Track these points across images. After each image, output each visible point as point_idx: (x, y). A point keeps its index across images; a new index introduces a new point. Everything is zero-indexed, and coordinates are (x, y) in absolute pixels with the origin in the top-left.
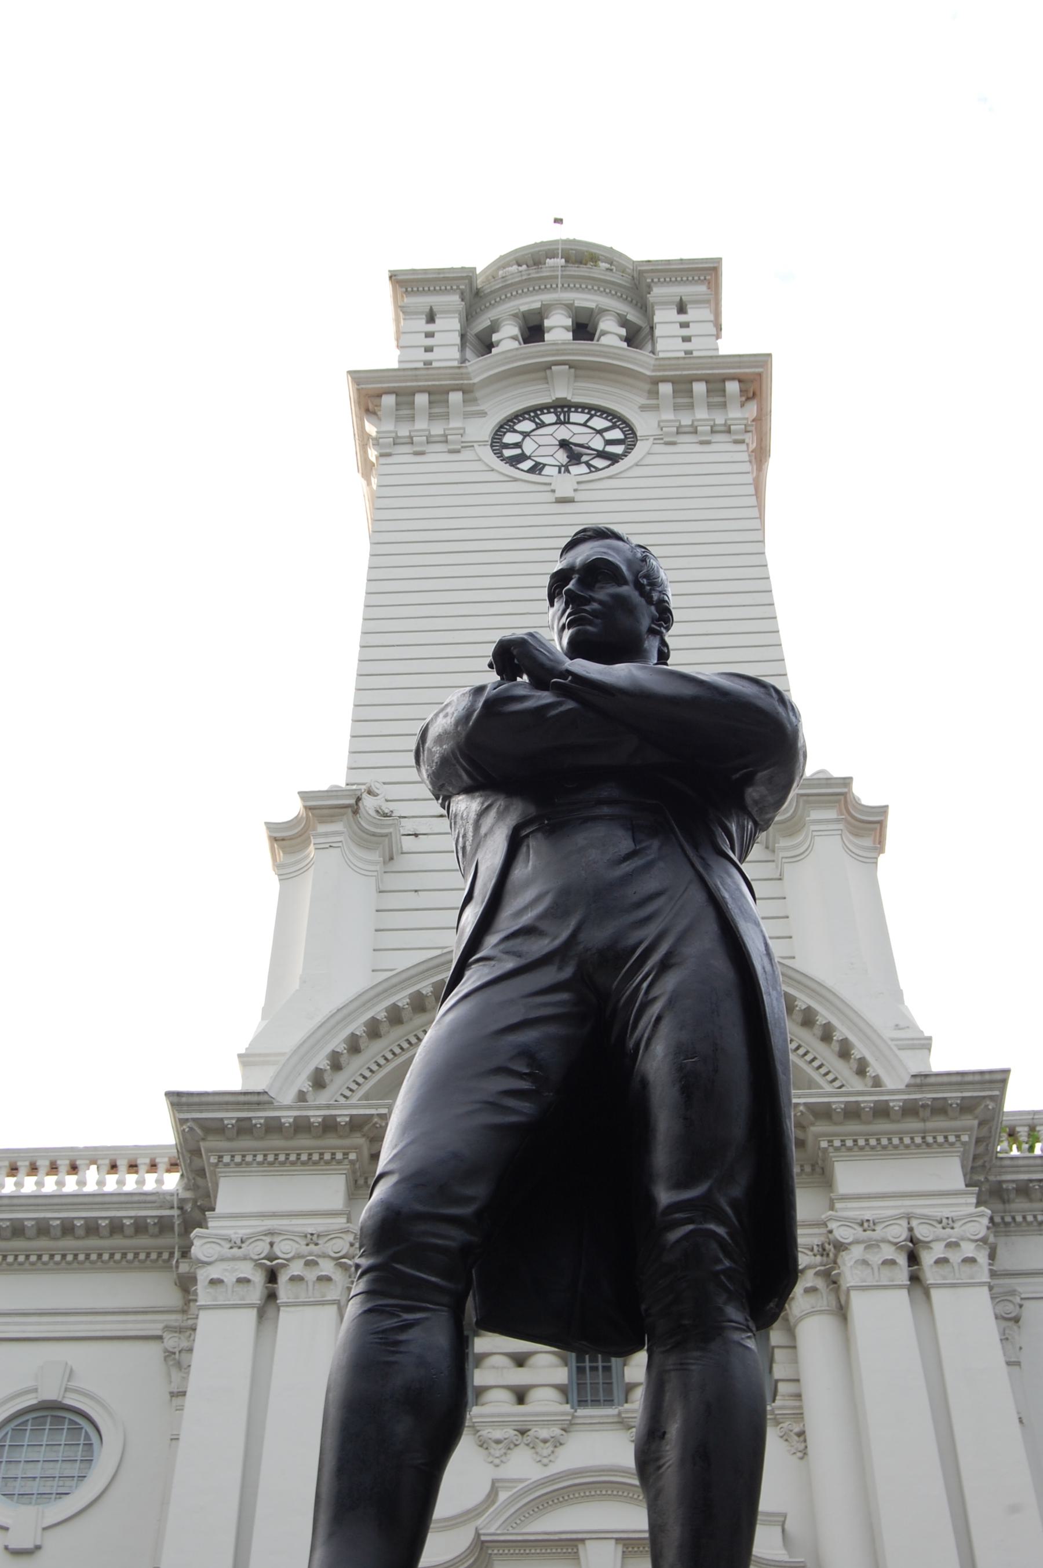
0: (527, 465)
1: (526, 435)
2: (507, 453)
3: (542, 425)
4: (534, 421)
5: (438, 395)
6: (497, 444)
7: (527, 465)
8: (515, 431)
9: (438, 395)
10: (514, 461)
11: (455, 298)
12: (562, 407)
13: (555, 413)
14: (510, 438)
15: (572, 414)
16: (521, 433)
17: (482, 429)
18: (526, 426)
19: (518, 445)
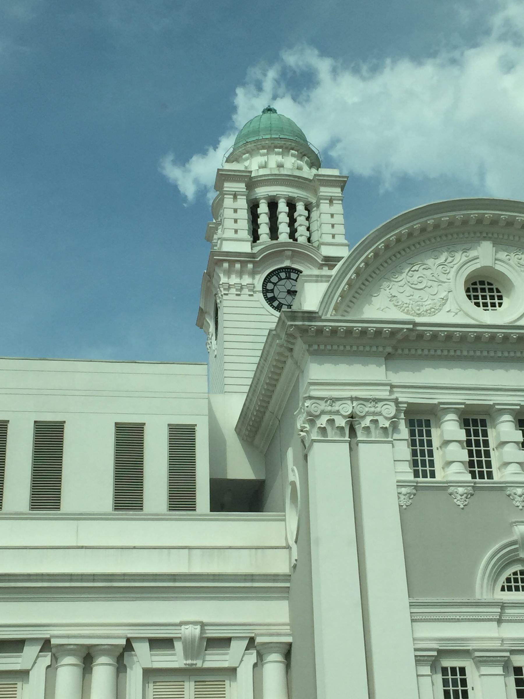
0: (276, 304)
1: (275, 284)
2: (270, 295)
3: (280, 279)
4: (277, 276)
5: (243, 264)
6: (265, 291)
7: (276, 304)
8: (271, 282)
9: (243, 264)
10: (270, 301)
11: (243, 185)
12: (288, 269)
13: (285, 272)
14: (270, 286)
15: (292, 274)
16: (273, 283)
17: (259, 281)
18: (274, 279)
19: (272, 291)
